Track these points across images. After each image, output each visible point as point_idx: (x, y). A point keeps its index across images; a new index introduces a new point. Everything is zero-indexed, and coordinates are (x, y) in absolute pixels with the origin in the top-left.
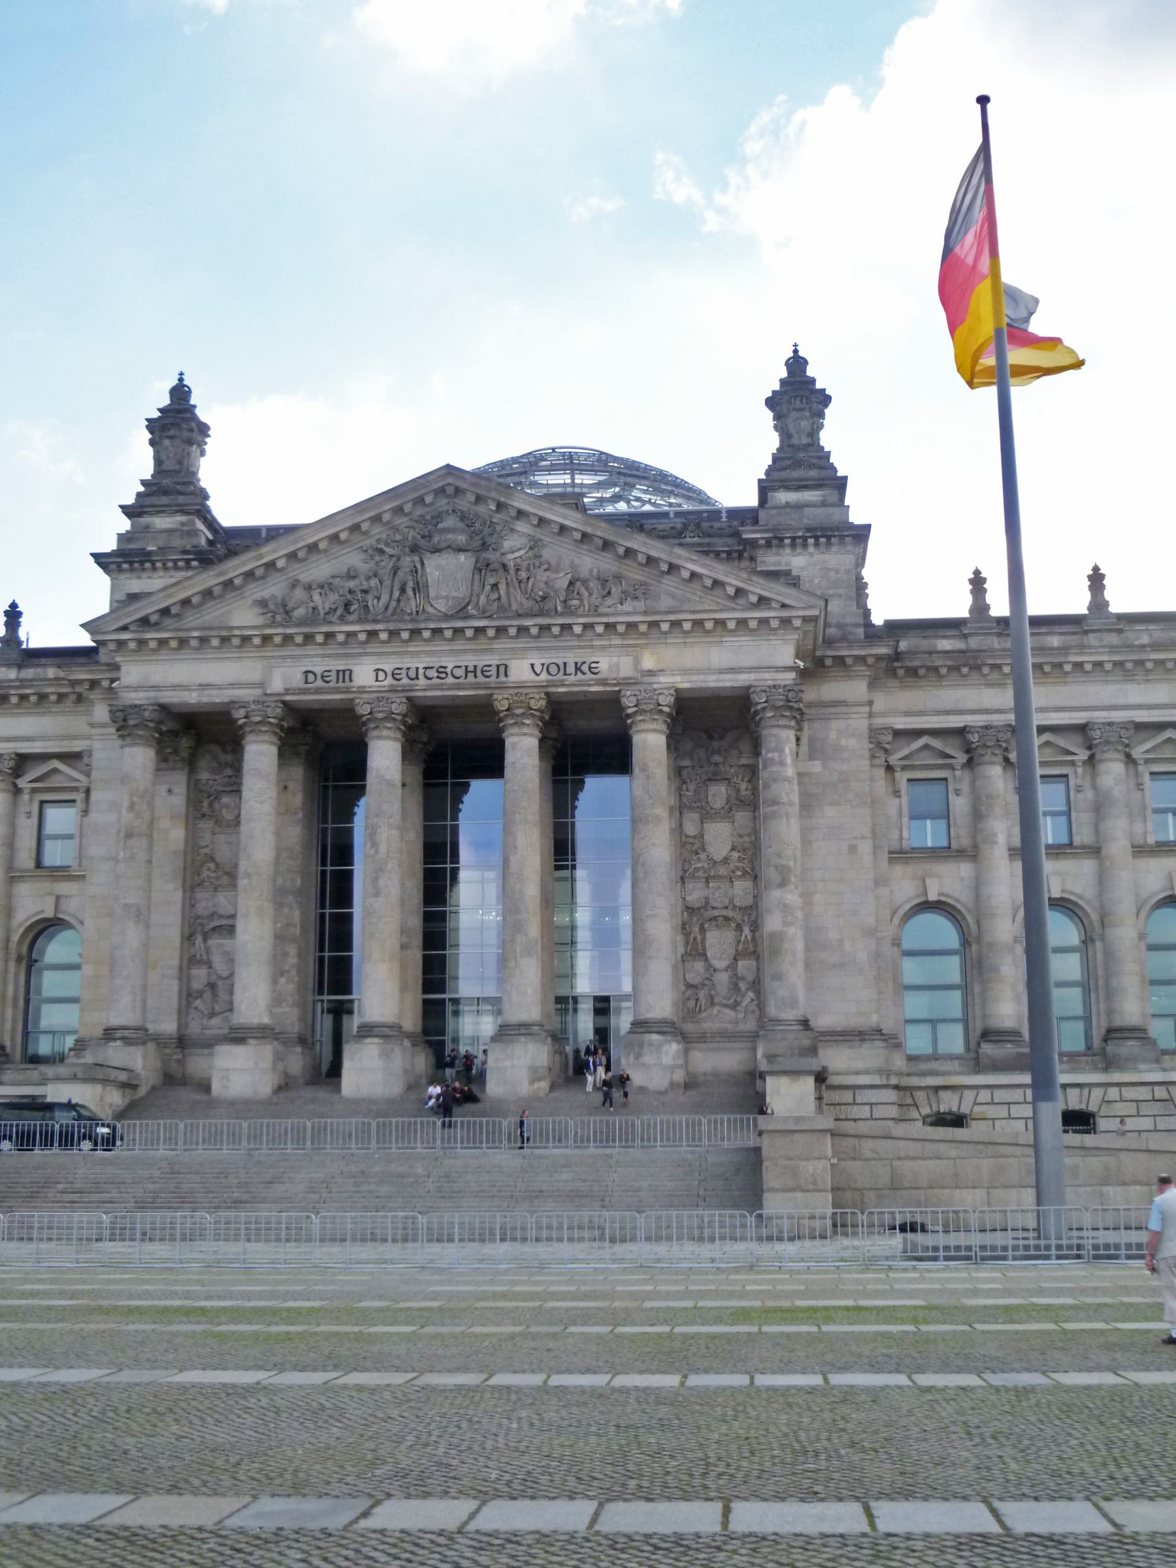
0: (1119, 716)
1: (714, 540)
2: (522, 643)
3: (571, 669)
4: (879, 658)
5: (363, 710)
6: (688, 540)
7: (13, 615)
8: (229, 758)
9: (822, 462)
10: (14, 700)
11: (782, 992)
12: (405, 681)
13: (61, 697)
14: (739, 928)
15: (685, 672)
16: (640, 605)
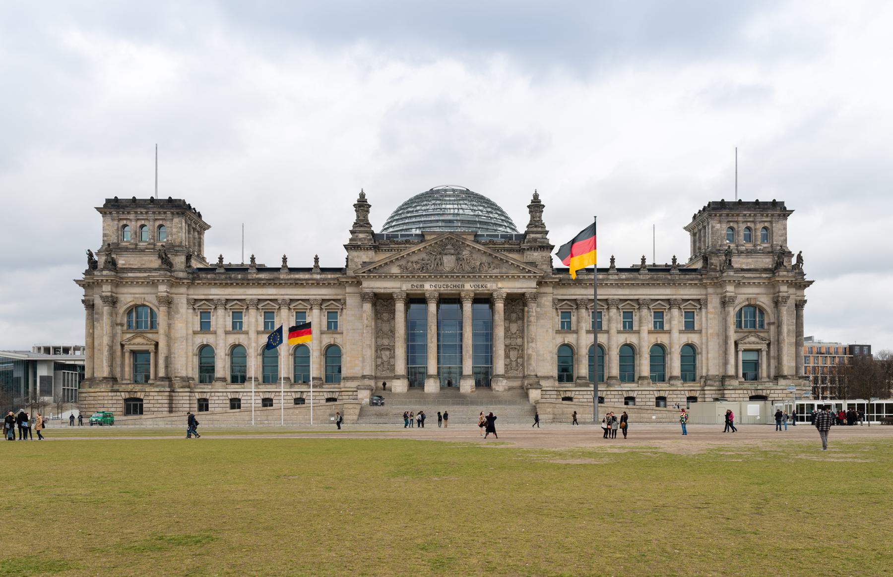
0: (616, 297)
1: (513, 246)
2: (468, 279)
3: (480, 286)
4: (556, 282)
5: (427, 295)
6: (506, 246)
7: (317, 259)
8: (385, 303)
9: (542, 226)
10: (321, 284)
11: (531, 368)
12: (438, 288)
13: (334, 284)
14: (518, 350)
15: (509, 288)
16: (498, 271)
